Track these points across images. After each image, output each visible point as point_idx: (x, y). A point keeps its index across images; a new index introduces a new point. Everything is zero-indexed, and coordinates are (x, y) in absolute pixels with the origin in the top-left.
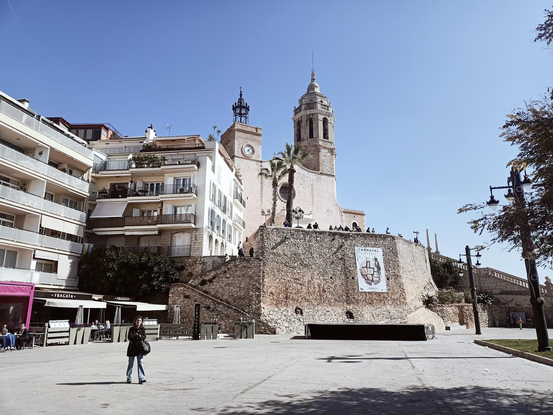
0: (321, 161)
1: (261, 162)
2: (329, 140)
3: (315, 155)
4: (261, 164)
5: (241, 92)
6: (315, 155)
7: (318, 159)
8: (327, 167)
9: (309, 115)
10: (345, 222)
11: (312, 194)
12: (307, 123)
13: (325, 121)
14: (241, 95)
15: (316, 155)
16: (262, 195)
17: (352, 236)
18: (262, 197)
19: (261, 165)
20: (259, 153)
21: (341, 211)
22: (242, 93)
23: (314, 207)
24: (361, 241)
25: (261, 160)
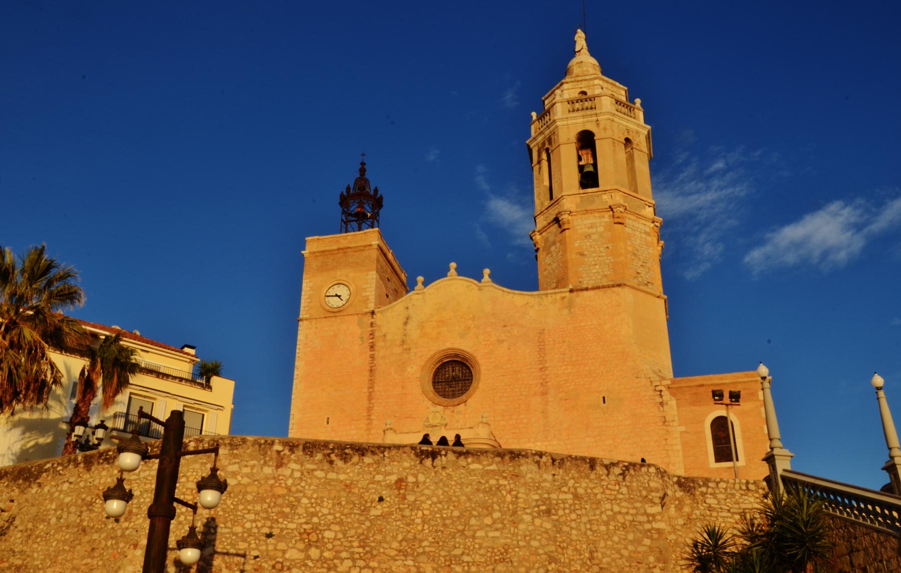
0: (572, 256)
1: (373, 313)
2: (601, 188)
3: (558, 245)
4: (373, 320)
5: (363, 164)
6: (558, 245)
7: (565, 251)
8: (597, 267)
9: (544, 144)
10: (676, 423)
12: (540, 168)
13: (586, 140)
14: (363, 171)
15: (561, 244)
16: (372, 402)
17: (46, 471)
18: (369, 410)
19: (372, 324)
20: (367, 294)
21: (659, 388)
22: (365, 167)
23: (550, 399)
24: (71, 483)
25: (371, 307)
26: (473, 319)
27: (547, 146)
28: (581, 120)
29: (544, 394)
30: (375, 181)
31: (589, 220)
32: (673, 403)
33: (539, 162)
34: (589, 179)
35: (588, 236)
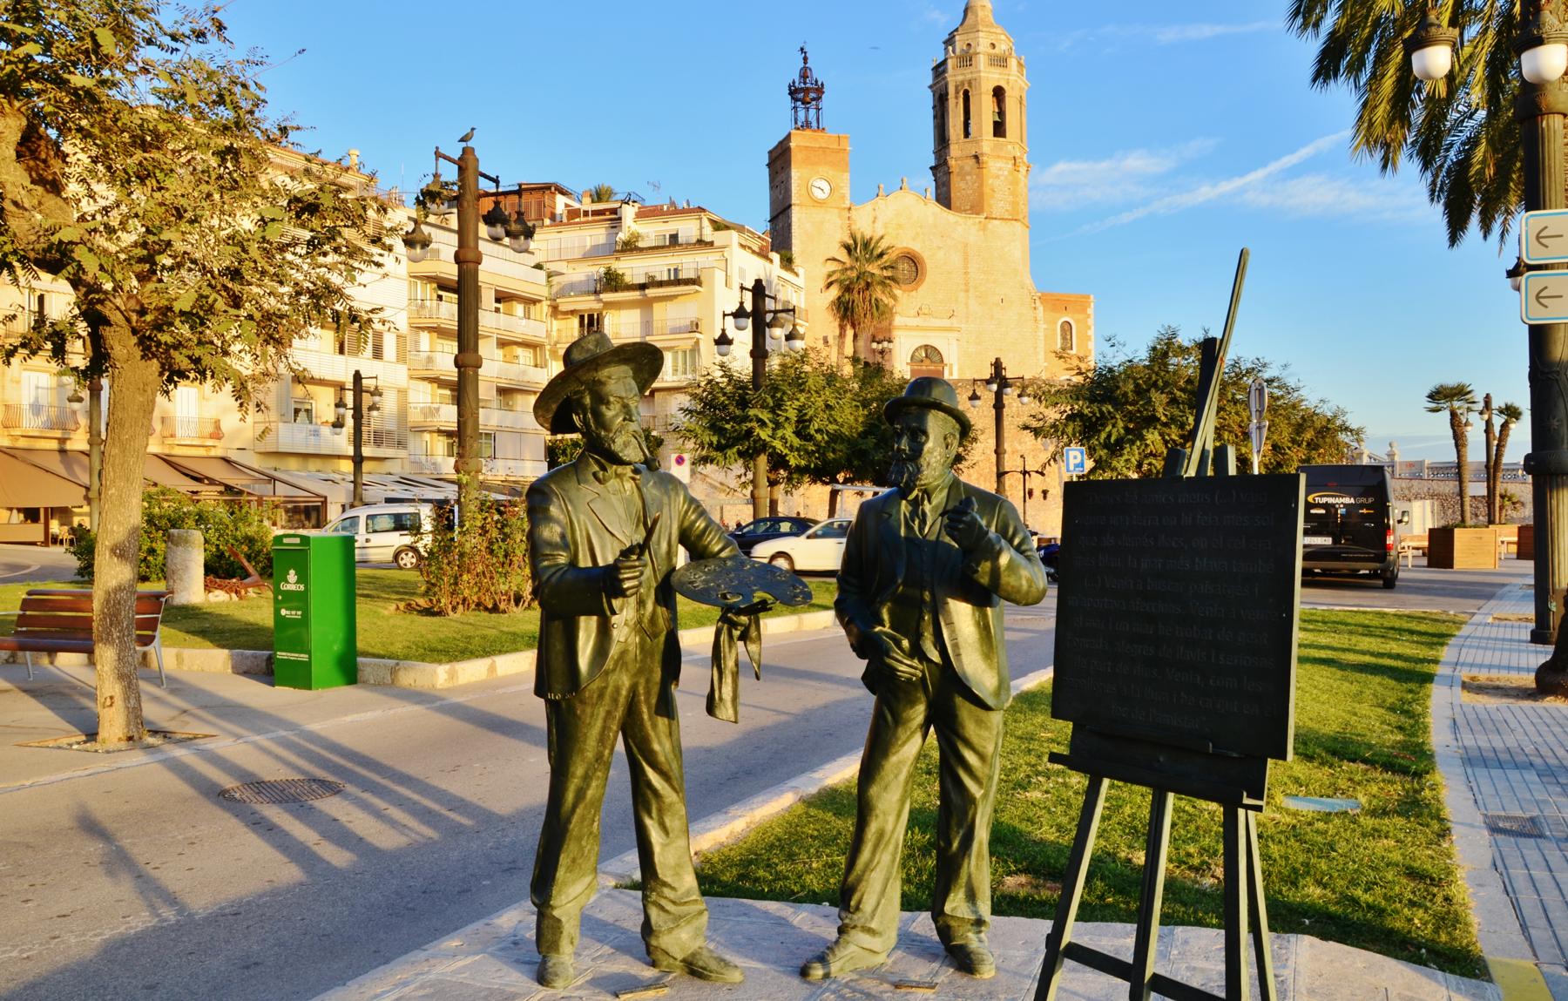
0: (987, 190)
7: (981, 185)
9: (963, 83)
11: (966, 267)
13: (999, 93)
14: (805, 59)
25: (847, 203)
26: (921, 227)
27: (966, 87)
28: (997, 76)
29: (967, 291)
30: (818, 74)
31: (1000, 164)
32: (1041, 308)
33: (956, 98)
34: (999, 129)
35: (998, 177)
